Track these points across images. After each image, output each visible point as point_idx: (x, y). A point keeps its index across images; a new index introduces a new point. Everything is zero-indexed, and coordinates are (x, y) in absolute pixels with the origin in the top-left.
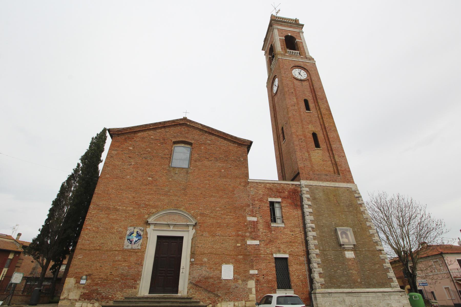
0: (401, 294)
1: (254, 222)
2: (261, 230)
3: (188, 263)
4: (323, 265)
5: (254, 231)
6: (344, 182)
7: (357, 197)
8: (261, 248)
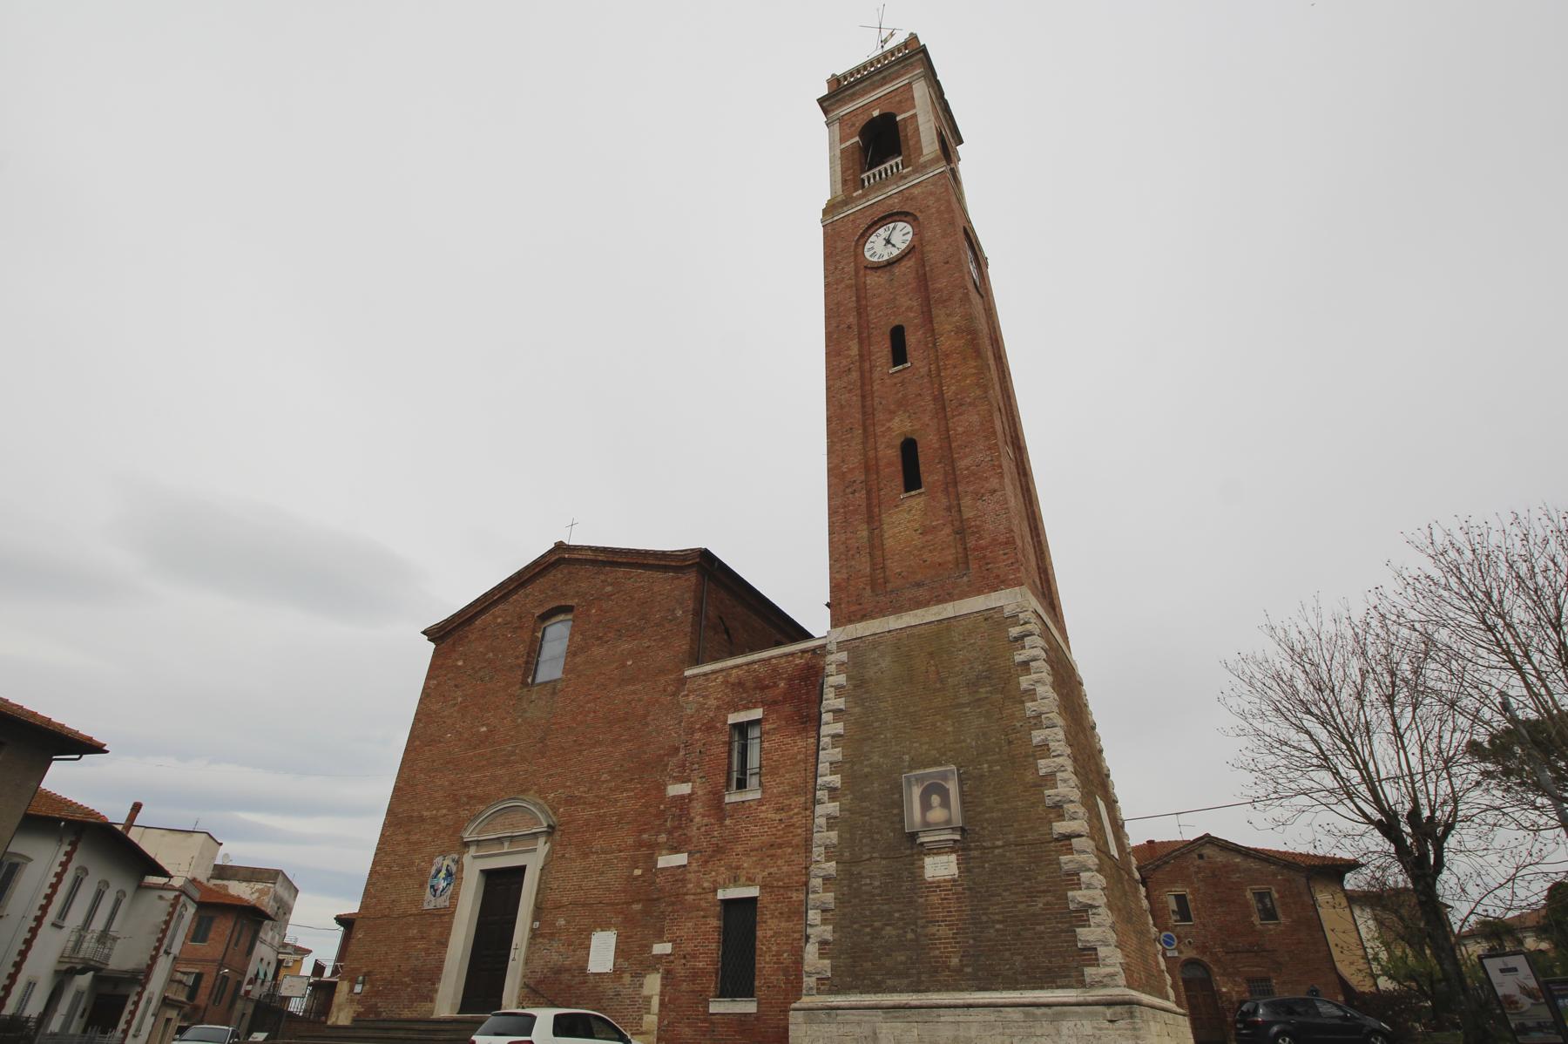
0: (1109, 1012)
1: (682, 797)
2: (698, 819)
3: (527, 934)
4: (839, 917)
5: (679, 827)
6: (979, 592)
7: (1016, 639)
8: (689, 876)
